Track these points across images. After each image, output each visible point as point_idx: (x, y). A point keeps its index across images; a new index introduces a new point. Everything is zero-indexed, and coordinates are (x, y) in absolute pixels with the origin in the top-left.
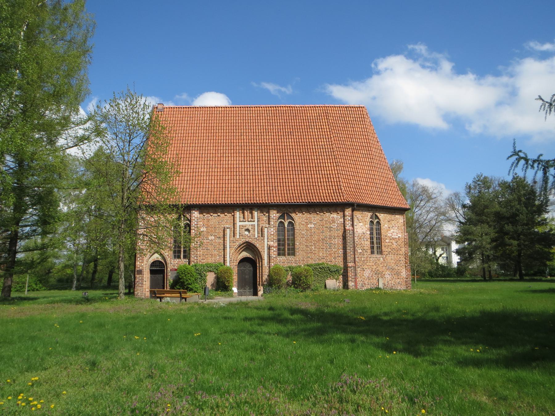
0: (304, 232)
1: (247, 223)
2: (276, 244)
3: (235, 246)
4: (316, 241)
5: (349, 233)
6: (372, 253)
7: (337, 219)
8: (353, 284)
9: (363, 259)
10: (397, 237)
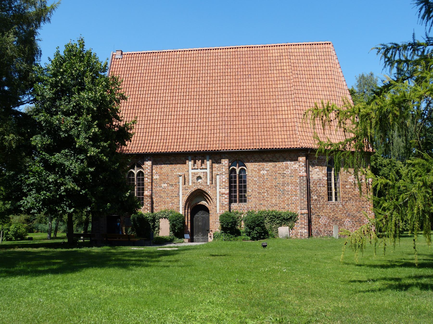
1: (199, 170)
2: (228, 191)
3: (187, 193)
4: (269, 187)
5: (303, 179)
6: (330, 199)
7: (290, 165)
8: (306, 231)
9: (318, 206)
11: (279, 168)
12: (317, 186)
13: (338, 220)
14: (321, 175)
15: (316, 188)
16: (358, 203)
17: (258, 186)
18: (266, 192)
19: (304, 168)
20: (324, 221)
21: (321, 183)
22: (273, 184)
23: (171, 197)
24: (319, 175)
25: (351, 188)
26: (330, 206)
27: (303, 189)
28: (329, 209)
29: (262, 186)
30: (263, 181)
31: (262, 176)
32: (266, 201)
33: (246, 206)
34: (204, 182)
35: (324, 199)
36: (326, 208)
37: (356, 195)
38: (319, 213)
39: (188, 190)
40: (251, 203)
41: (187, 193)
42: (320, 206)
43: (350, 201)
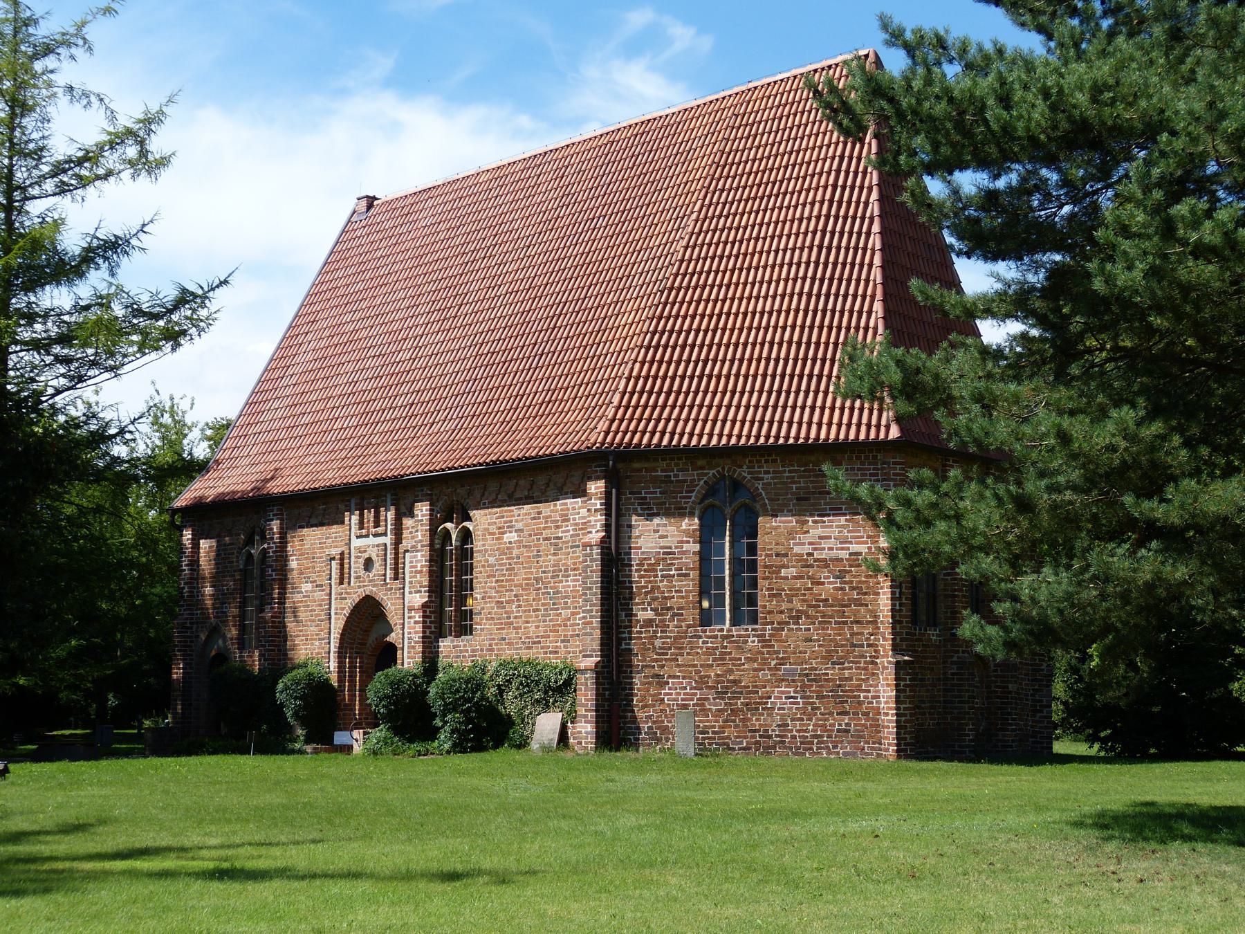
0: (492, 560)
3: (343, 609)
4: (520, 585)
5: (591, 554)
7: (574, 509)
9: (658, 643)
10: (844, 554)
11: (546, 522)
12: (656, 576)
13: (741, 693)
14: (673, 536)
15: (650, 582)
16: (833, 629)
17: (497, 581)
18: (513, 601)
19: (599, 517)
20: (679, 694)
21: (673, 564)
22: (531, 573)
24: (666, 537)
25: (801, 577)
26: (704, 642)
27: (590, 588)
28: (704, 654)
29: (507, 581)
30: (510, 564)
31: (508, 548)
32: (515, 628)
33: (471, 645)
35: (684, 620)
36: (691, 649)
37: (827, 600)
38: (663, 666)
40: (480, 634)
41: (343, 609)
42: (663, 643)
43: (798, 623)
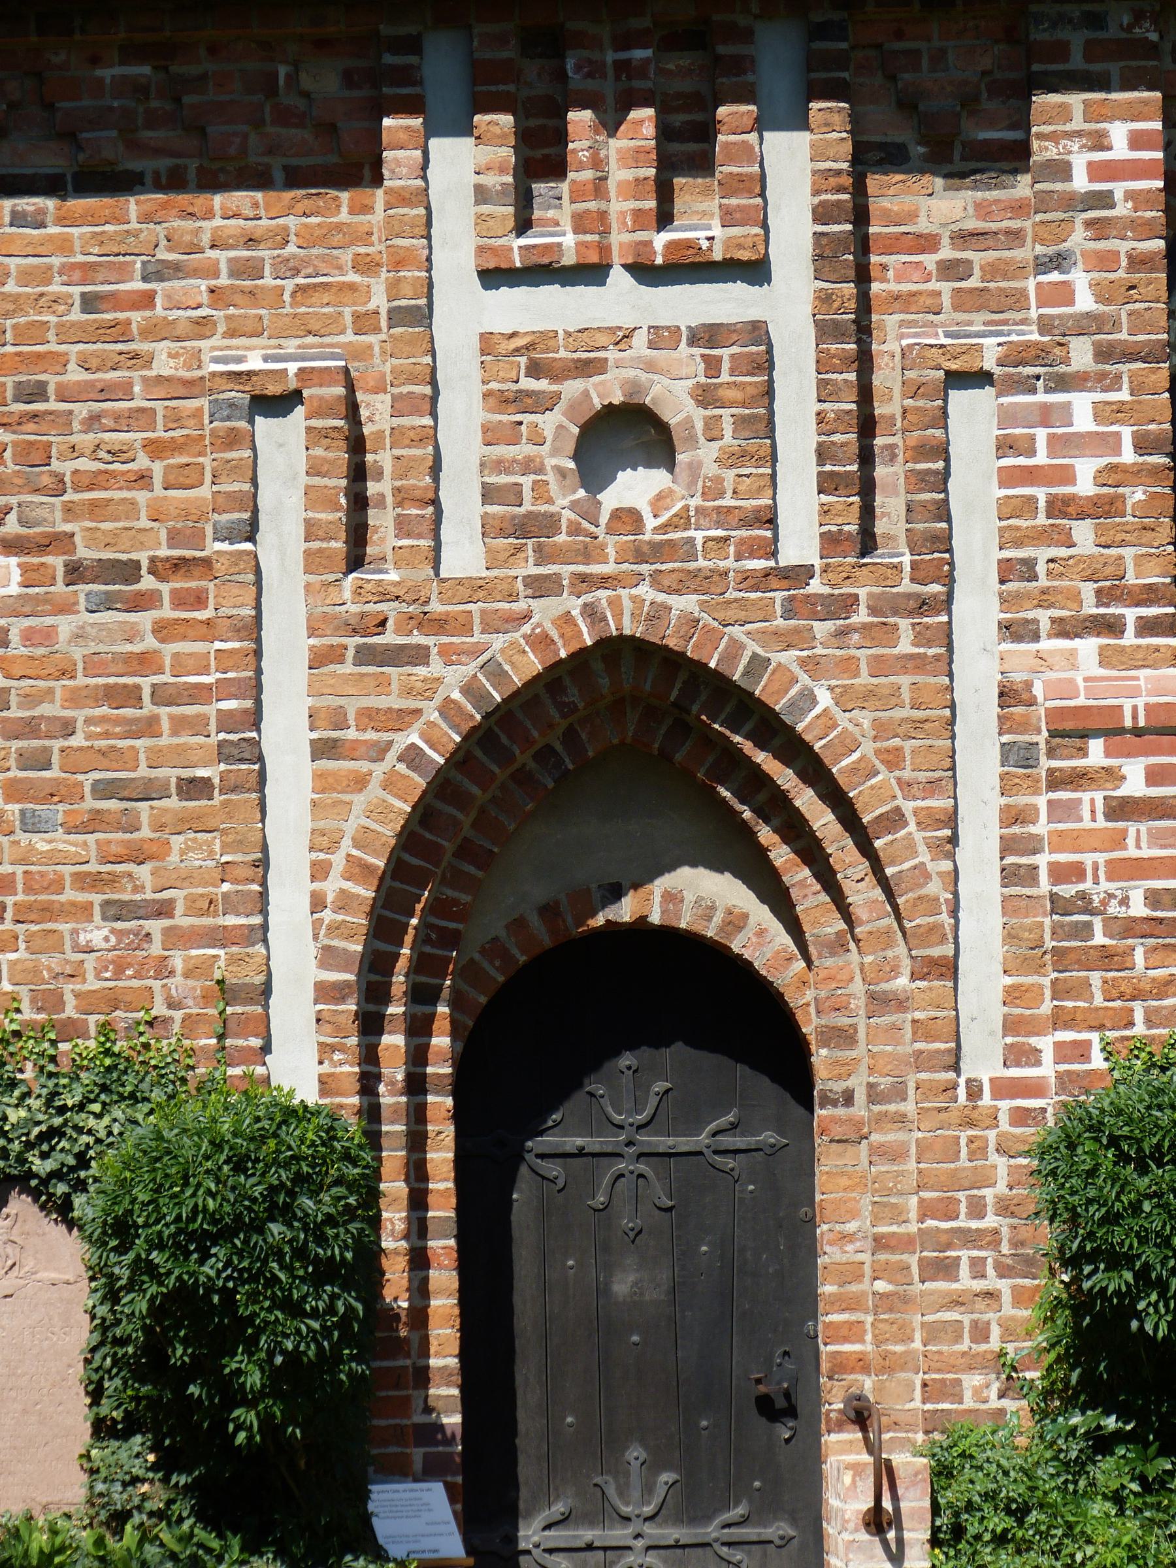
3: (402, 719)
23: (104, 790)
34: (723, 516)
39: (420, 656)
41: (402, 719)
